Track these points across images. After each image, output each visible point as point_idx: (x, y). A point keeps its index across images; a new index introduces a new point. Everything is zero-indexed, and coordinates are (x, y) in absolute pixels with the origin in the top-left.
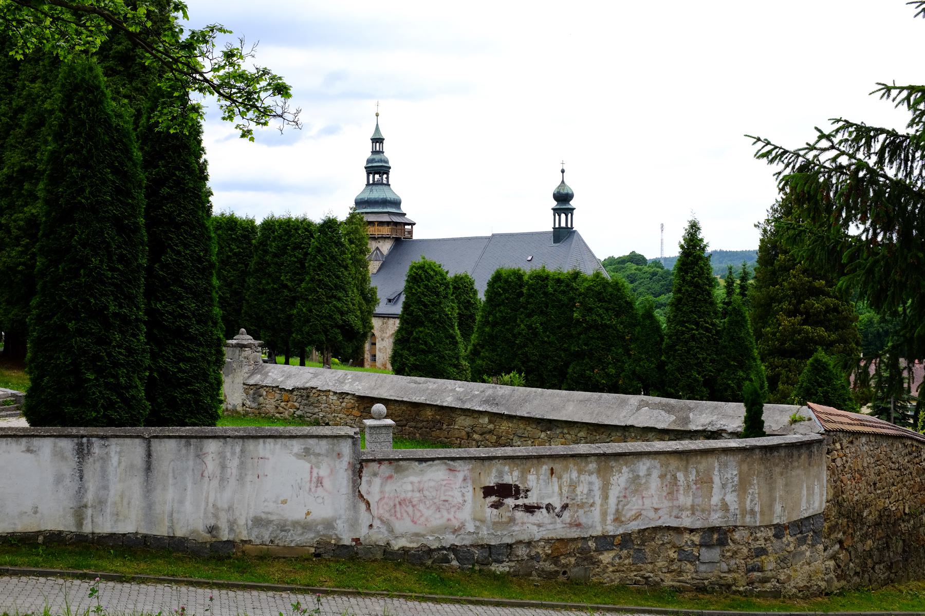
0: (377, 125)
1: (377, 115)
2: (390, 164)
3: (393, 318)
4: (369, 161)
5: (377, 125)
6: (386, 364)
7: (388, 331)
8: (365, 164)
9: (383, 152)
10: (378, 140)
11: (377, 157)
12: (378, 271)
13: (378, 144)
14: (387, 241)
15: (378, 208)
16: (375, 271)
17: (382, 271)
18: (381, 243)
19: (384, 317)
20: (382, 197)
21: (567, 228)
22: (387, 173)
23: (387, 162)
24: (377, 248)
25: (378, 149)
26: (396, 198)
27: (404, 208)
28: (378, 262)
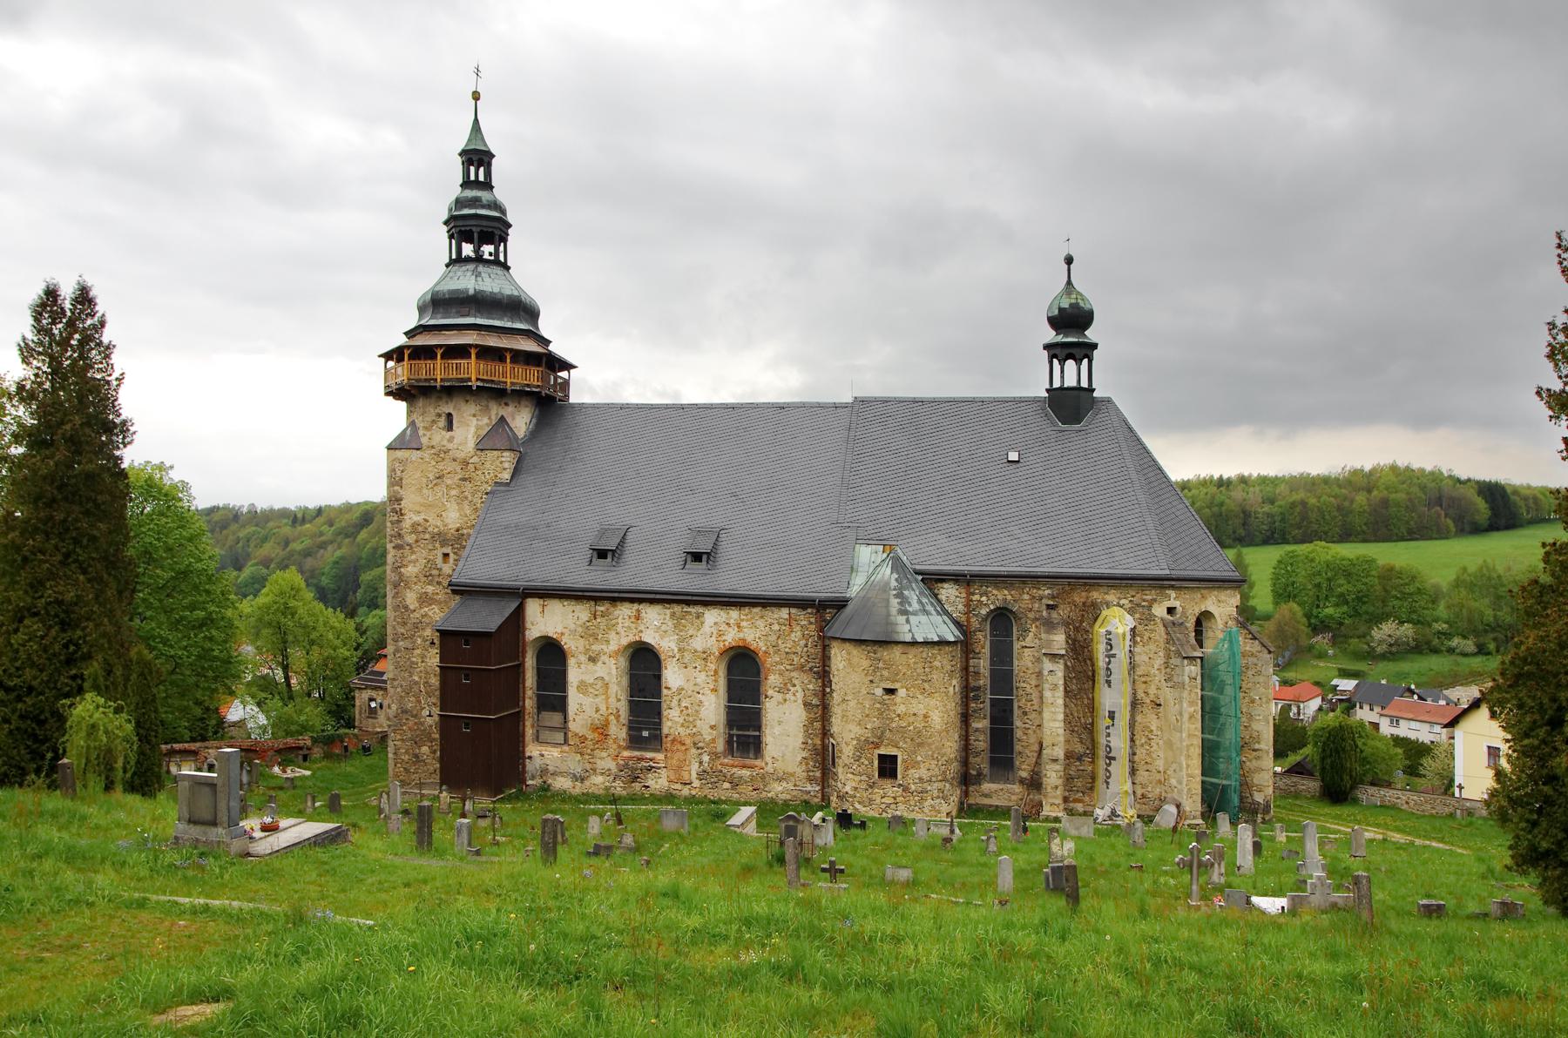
0: (476, 120)
2: (510, 218)
3: (632, 601)
5: (476, 120)
6: (606, 724)
7: (612, 635)
9: (492, 188)
10: (477, 157)
13: (472, 169)
16: (506, 476)
17: (526, 479)
18: (510, 409)
19: (596, 600)
21: (1079, 389)
22: (504, 239)
24: (502, 419)
25: (481, 178)
27: (545, 328)
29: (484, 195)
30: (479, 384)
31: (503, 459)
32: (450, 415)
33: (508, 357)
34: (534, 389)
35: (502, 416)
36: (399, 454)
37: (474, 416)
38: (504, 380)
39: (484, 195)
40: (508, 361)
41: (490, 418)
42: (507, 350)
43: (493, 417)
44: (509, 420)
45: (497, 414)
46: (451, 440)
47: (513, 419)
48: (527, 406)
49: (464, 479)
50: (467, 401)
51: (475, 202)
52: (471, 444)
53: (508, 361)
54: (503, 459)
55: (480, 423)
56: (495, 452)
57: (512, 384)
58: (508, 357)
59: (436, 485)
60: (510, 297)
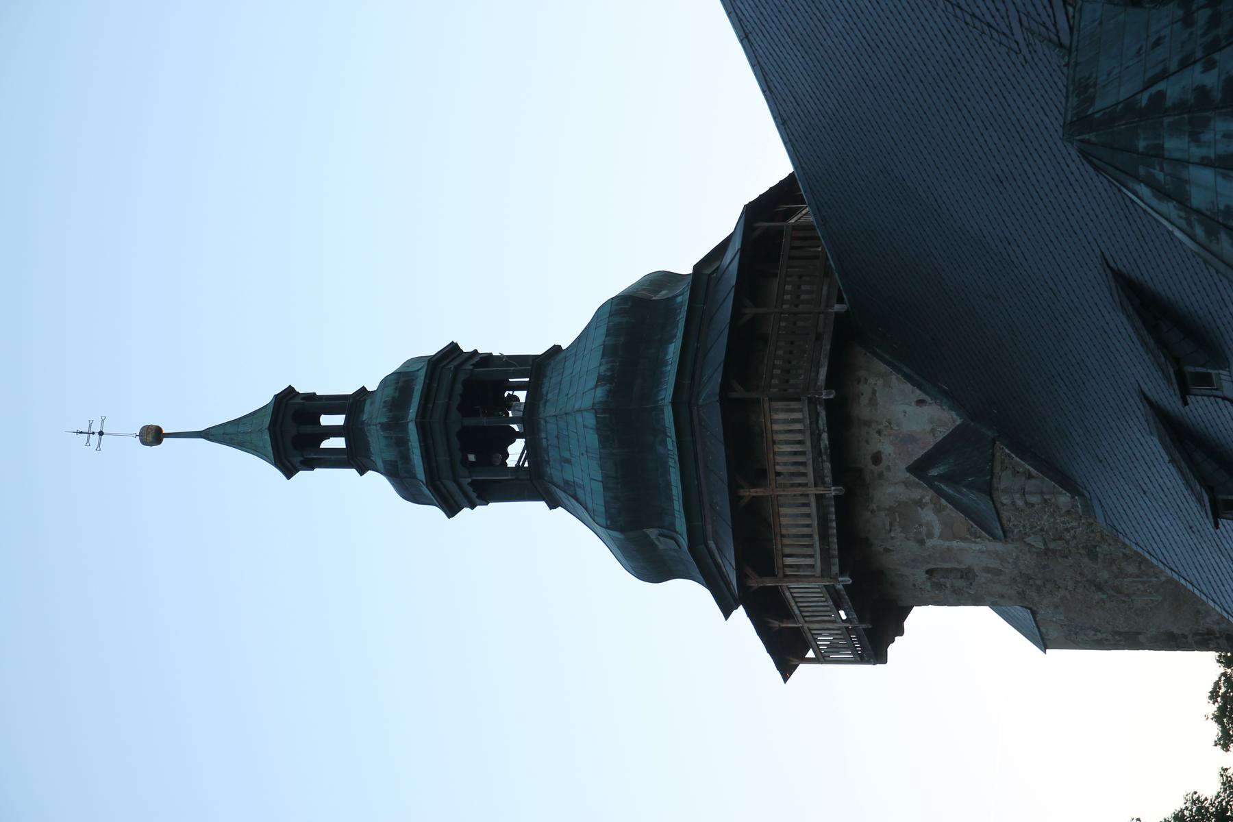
0: (208, 434)
1: (153, 436)
4: (410, 493)
5: (208, 434)
8: (434, 513)
11: (377, 442)
12: (1068, 483)
14: (863, 410)
15: (666, 472)
16: (1064, 499)
18: (887, 448)
20: (593, 439)
23: (400, 381)
24: (919, 468)
26: (600, 337)
28: (1004, 481)
29: (374, 415)
30: (835, 569)
31: (1020, 503)
32: (930, 572)
33: (754, 492)
34: (823, 422)
35: (913, 469)
36: (1053, 634)
37: (921, 542)
38: (813, 500)
39: (374, 415)
40: (759, 492)
41: (920, 503)
42: (734, 499)
43: (916, 494)
44: (918, 452)
45: (906, 484)
46: (998, 572)
47: (911, 438)
48: (873, 402)
49: (1092, 554)
50: (887, 550)
51: (395, 425)
52: (998, 546)
53: (759, 492)
54: (1020, 503)
55: (937, 531)
56: (1005, 515)
57: (819, 480)
58: (754, 492)
59: (1119, 591)
60: (604, 440)
